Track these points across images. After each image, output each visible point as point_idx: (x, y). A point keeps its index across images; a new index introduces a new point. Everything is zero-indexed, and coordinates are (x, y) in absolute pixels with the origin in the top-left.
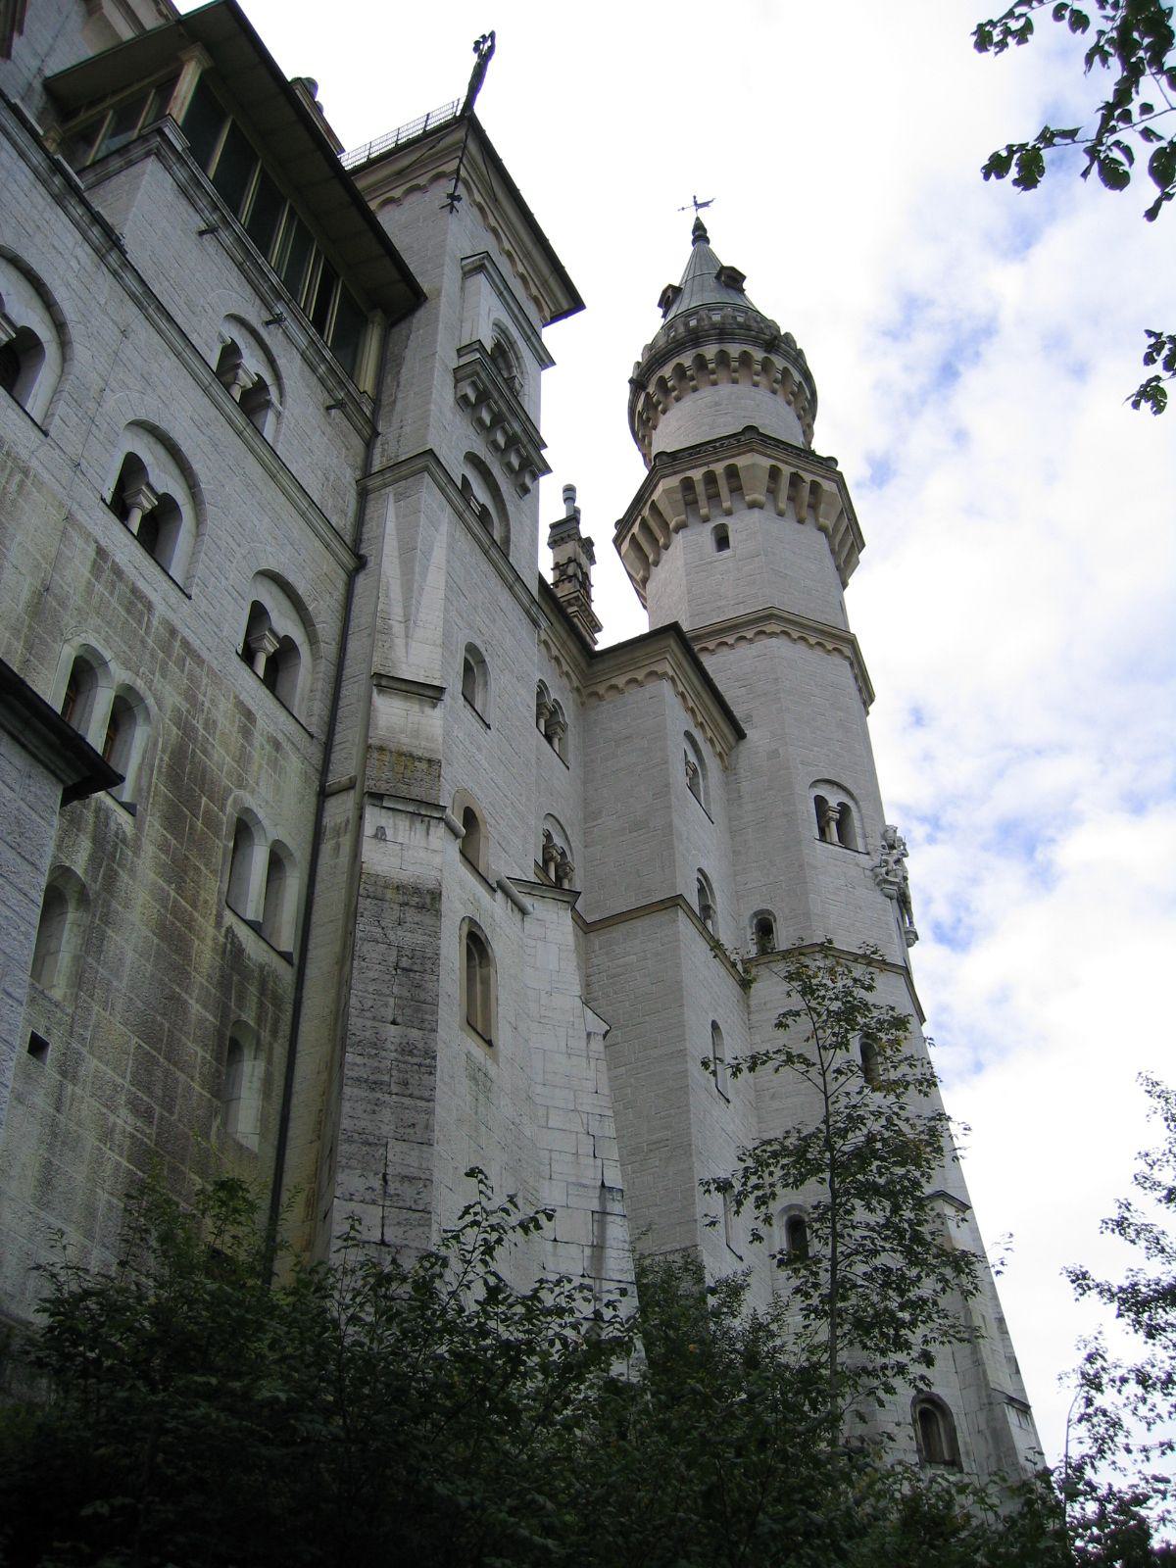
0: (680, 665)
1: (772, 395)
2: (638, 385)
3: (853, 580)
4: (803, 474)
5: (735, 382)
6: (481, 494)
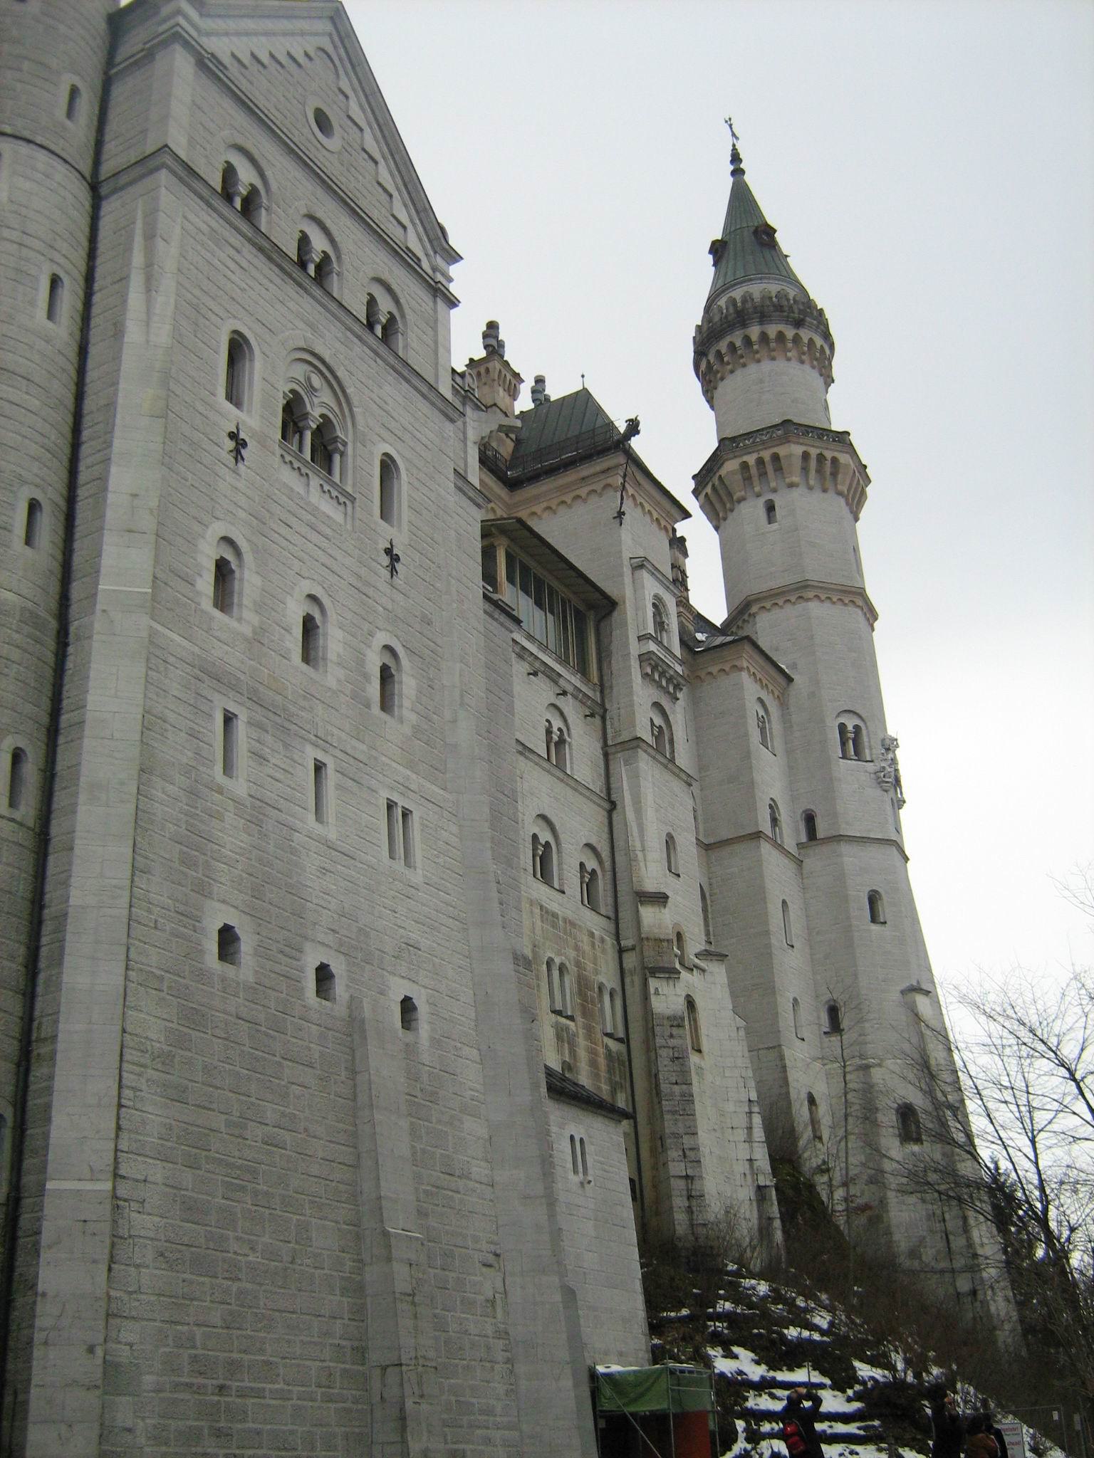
0: (751, 657)
2: (700, 353)
3: (861, 515)
5: (773, 359)
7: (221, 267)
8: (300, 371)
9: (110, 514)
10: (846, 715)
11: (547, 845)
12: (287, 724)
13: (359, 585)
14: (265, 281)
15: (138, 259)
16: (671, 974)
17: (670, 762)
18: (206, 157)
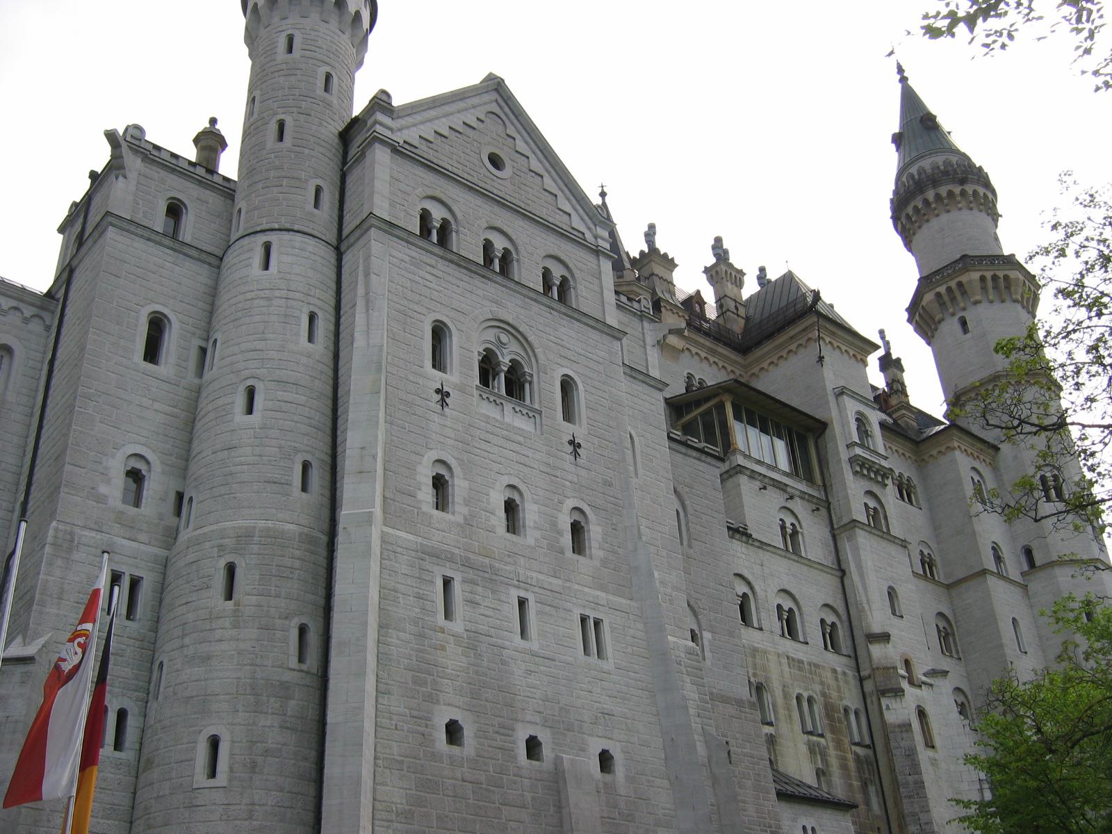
0: (960, 438)
2: (896, 218)
4: (998, 273)
5: (948, 211)
7: (420, 280)
8: (490, 335)
9: (347, 463)
11: (791, 610)
12: (494, 577)
13: (548, 470)
14: (454, 281)
15: (361, 290)
16: (898, 693)
17: (887, 536)
18: (405, 211)
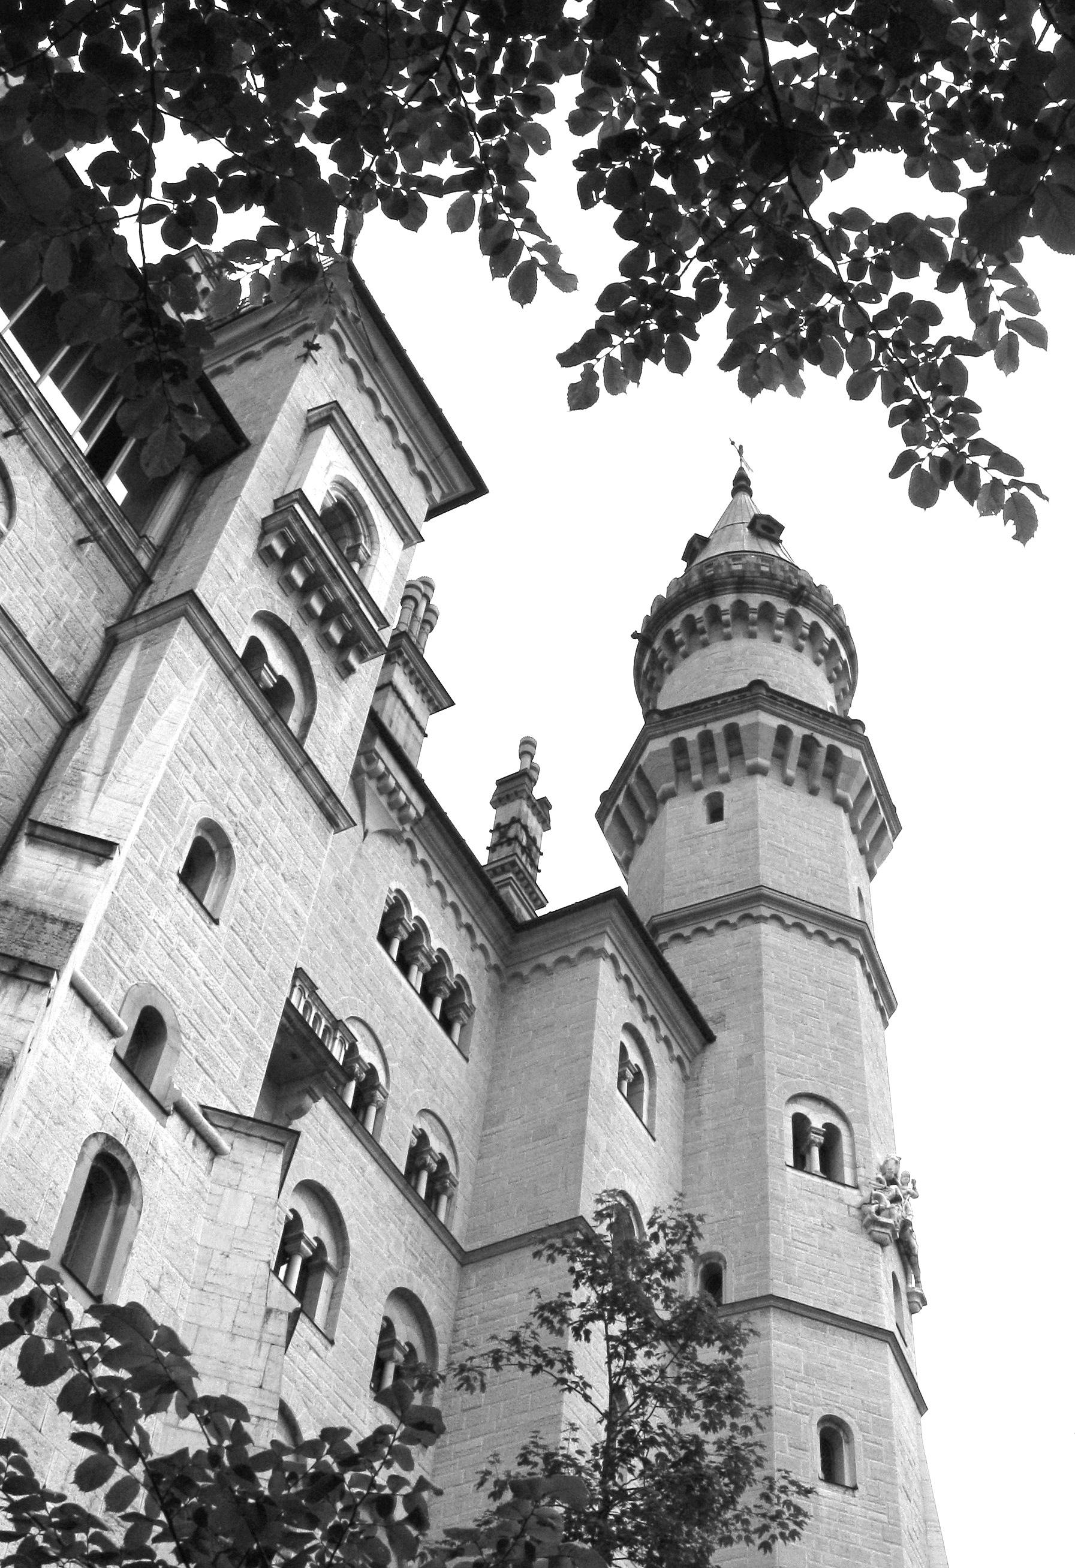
0: (624, 943)
1: (796, 653)
2: (643, 641)
4: (819, 737)
5: (752, 635)
6: (278, 662)
10: (812, 1104)
